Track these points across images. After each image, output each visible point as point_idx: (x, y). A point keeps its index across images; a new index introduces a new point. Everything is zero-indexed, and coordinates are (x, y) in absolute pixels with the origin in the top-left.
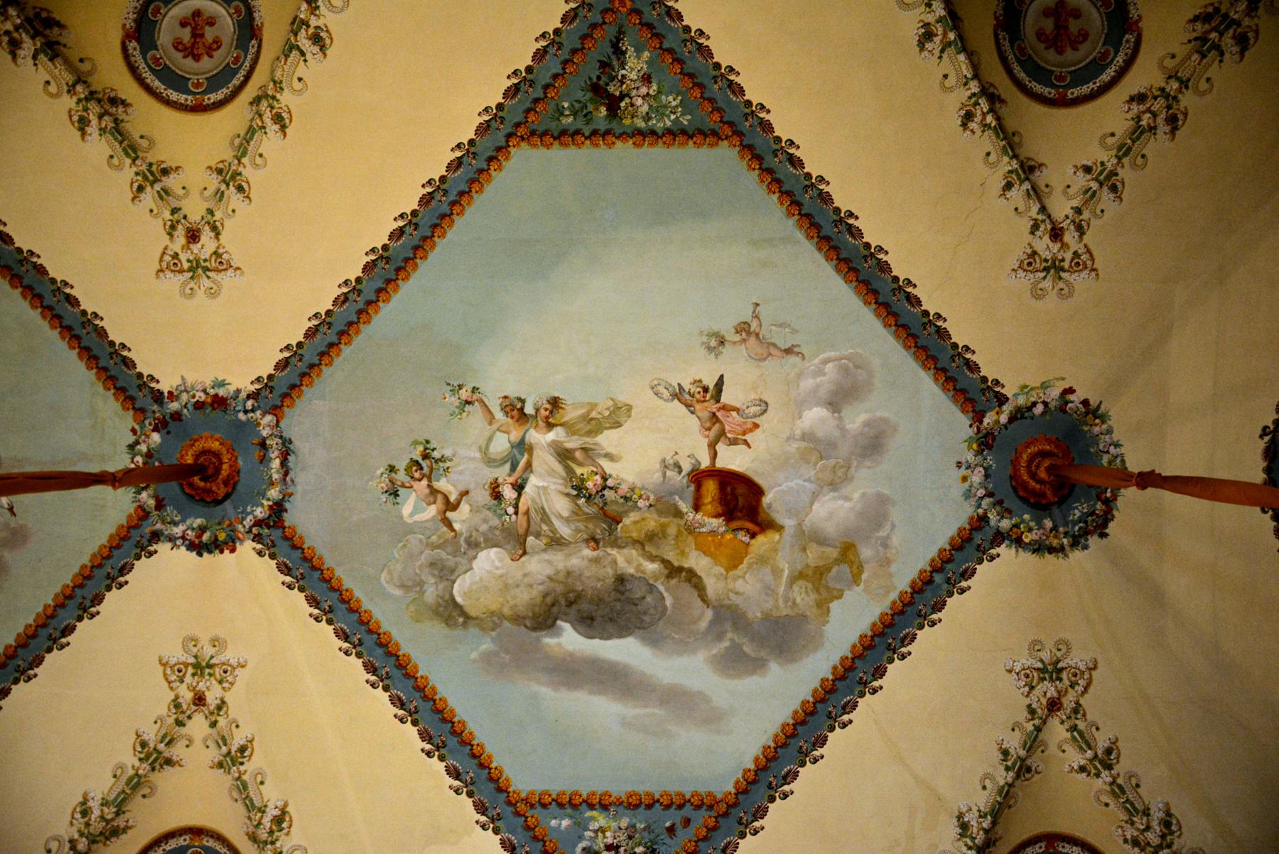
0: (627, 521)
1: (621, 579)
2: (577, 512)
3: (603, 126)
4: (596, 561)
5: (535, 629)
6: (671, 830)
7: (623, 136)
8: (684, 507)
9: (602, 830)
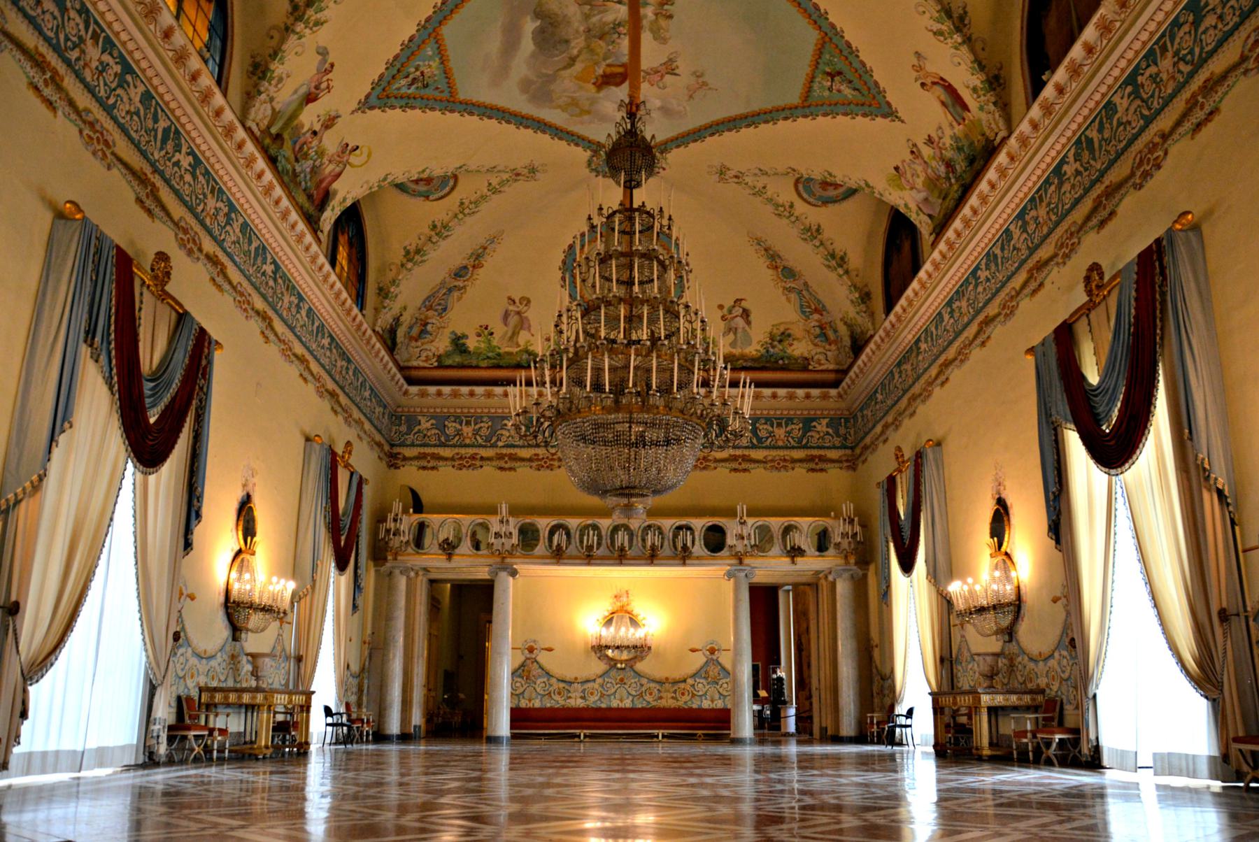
0: (601, 42)
1: (567, 42)
2: (605, 24)
3: (820, 66)
4: (577, 31)
5: (535, 12)
6: (437, 88)
7: (814, 71)
8: (608, 62)
9: (430, 66)
